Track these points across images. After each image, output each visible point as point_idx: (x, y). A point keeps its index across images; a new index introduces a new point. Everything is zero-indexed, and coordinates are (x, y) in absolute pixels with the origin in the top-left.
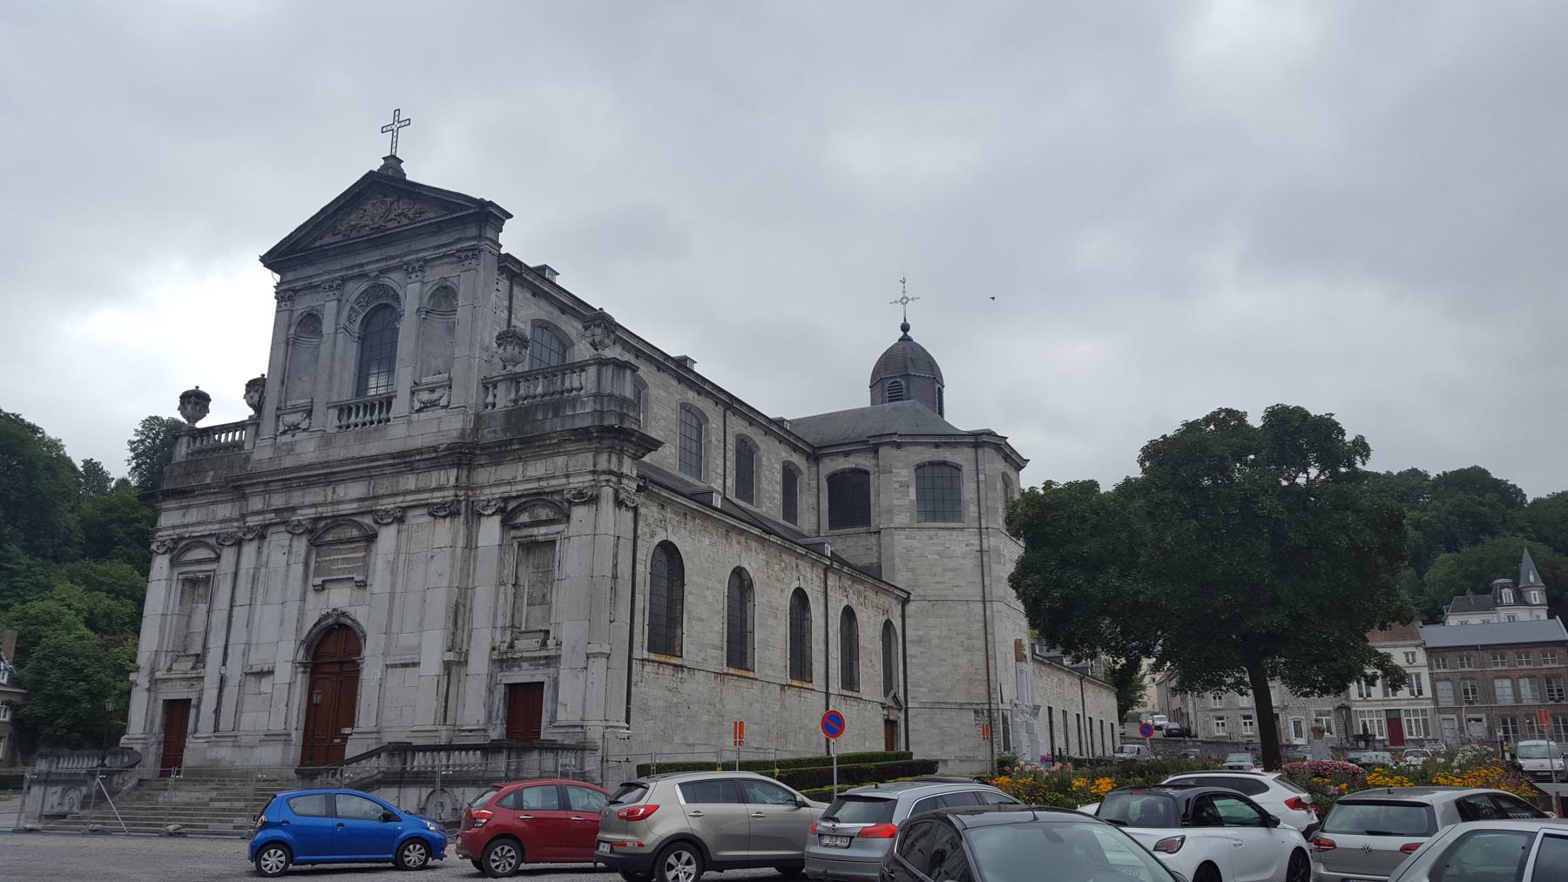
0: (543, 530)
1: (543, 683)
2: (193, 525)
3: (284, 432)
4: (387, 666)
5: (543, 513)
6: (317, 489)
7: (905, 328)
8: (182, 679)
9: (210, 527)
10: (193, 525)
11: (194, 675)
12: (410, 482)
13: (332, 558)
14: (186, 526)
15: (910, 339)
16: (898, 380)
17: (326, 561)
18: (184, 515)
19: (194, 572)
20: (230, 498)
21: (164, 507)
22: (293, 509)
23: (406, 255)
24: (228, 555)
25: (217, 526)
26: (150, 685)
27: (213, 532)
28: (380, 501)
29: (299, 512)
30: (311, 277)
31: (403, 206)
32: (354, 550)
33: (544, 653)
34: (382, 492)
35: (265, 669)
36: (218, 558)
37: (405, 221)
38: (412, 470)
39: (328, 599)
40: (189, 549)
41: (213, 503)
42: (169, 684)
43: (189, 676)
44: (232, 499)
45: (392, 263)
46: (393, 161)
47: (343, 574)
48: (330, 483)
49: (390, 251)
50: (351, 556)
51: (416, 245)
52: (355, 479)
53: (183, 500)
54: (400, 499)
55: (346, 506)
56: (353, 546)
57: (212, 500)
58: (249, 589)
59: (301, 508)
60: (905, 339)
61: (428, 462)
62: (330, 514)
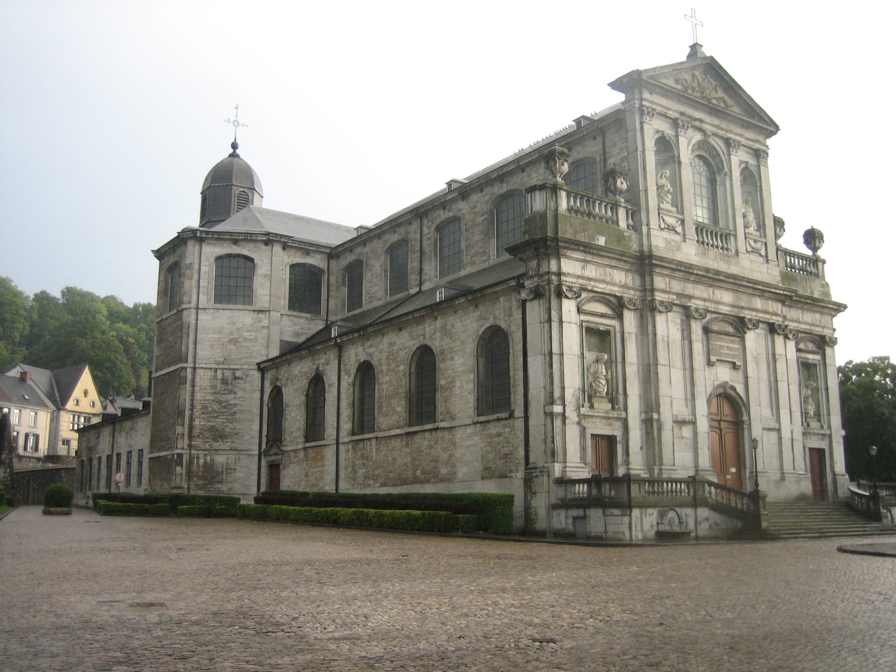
0: (810, 356)
1: (824, 450)
2: (595, 280)
3: (662, 229)
4: (764, 429)
5: (811, 346)
6: (702, 287)
7: (234, 146)
8: (603, 418)
9: (612, 288)
10: (595, 280)
11: (615, 416)
12: (758, 303)
13: (720, 343)
14: (589, 279)
15: (238, 156)
16: (245, 190)
17: (716, 345)
18: (583, 268)
19: (597, 324)
20: (628, 268)
21: (568, 254)
22: (690, 297)
23: (731, 131)
24: (630, 318)
25: (616, 289)
26: (580, 420)
27: (613, 293)
28: (743, 311)
29: (693, 300)
30: (668, 109)
31: (721, 94)
32: (733, 342)
33: (822, 432)
34: (743, 304)
35: (687, 420)
36: (620, 317)
37: (722, 105)
38: (760, 296)
39: (717, 373)
40: (590, 301)
41: (612, 267)
42: (590, 420)
43: (611, 415)
44: (628, 270)
45: (721, 133)
46: (695, 48)
47: (728, 357)
48: (711, 286)
49: (724, 125)
50: (731, 345)
51: (731, 127)
52: (727, 289)
53: (589, 256)
54: (754, 313)
55: (721, 307)
56: (731, 338)
57: (613, 264)
58: (667, 353)
59: (696, 298)
60: (234, 155)
61: (772, 295)
62: (713, 310)
